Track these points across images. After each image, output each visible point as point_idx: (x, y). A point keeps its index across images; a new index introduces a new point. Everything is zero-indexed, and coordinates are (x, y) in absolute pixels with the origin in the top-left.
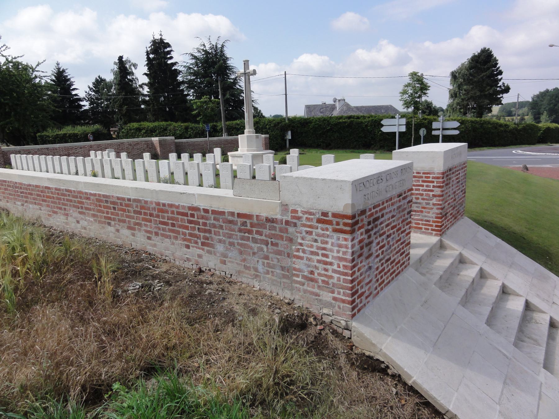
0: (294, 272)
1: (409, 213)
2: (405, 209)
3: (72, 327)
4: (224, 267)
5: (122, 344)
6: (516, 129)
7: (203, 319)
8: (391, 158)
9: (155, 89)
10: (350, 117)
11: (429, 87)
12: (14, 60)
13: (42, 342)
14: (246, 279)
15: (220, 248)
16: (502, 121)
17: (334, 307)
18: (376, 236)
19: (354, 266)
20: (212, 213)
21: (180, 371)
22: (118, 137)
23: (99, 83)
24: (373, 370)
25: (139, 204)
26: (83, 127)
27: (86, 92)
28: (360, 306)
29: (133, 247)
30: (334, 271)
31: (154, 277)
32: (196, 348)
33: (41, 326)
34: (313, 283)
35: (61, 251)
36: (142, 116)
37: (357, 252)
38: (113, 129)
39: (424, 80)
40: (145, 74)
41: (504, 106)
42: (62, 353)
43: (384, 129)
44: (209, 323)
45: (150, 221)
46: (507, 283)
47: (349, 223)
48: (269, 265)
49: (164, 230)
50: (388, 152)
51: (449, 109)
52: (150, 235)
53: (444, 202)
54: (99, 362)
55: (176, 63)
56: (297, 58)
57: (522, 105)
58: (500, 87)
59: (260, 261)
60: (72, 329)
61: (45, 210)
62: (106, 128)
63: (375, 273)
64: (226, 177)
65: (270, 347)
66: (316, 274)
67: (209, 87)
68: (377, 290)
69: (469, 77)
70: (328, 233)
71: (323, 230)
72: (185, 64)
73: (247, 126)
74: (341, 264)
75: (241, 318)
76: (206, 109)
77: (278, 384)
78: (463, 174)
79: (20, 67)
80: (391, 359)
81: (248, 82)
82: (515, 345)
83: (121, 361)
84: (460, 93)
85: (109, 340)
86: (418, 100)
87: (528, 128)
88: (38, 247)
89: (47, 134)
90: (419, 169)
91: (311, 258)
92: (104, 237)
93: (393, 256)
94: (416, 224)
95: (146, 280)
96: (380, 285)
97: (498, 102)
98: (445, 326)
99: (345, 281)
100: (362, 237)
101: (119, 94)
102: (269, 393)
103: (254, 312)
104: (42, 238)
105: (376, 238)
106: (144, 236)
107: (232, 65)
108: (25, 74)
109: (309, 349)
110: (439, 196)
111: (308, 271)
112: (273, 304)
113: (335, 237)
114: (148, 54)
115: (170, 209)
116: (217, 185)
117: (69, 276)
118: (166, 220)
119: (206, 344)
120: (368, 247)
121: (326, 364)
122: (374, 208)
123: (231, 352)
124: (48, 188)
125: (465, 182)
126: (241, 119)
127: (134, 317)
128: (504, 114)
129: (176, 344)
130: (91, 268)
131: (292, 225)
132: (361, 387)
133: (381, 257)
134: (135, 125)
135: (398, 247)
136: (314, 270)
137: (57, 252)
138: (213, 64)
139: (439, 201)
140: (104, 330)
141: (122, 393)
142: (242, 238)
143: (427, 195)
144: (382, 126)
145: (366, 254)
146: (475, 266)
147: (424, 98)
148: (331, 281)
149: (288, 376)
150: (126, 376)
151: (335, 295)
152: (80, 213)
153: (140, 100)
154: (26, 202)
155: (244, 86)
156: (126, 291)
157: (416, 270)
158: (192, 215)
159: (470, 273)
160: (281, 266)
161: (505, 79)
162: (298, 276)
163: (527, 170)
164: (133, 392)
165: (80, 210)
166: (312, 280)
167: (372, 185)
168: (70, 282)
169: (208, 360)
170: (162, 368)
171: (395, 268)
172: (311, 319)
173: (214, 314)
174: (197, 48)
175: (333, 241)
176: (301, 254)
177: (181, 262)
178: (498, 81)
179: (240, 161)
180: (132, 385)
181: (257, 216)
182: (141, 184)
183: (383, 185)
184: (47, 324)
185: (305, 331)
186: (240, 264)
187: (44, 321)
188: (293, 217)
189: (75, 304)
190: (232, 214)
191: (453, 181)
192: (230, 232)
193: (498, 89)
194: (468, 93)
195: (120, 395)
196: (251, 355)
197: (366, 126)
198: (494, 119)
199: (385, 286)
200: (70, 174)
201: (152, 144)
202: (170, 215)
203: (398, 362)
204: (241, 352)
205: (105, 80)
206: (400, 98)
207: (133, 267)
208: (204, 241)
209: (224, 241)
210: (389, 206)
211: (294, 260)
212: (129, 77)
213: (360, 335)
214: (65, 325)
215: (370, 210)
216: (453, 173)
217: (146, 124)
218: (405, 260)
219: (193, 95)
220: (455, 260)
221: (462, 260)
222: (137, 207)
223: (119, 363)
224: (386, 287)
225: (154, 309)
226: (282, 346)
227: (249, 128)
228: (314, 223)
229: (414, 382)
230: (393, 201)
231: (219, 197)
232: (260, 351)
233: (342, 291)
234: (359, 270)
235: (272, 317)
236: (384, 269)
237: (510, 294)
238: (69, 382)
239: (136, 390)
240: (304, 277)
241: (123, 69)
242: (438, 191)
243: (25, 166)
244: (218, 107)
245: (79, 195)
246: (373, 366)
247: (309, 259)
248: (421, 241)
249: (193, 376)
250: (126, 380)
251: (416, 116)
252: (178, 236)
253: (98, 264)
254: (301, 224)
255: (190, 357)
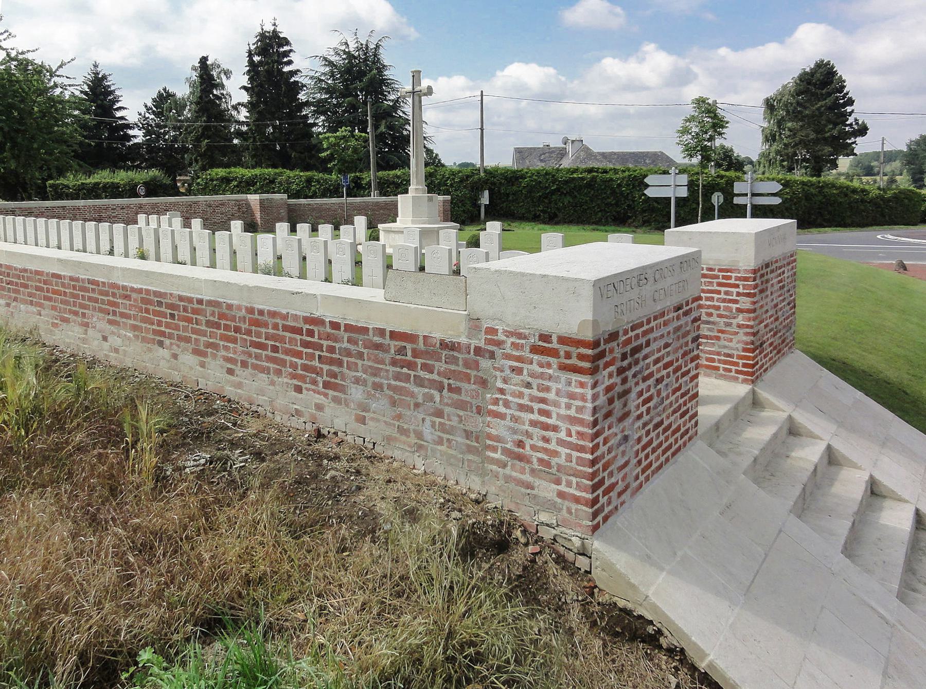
0: (489, 442)
1: (695, 339)
2: (688, 332)
3: (74, 536)
4: (361, 429)
5: (164, 571)
6: (882, 198)
7: (318, 527)
8: (662, 243)
9: (259, 112)
10: (590, 171)
11: (727, 123)
12: (20, 57)
13: (13, 564)
14: (399, 453)
15: (356, 393)
16: (856, 184)
17: (560, 510)
18: (636, 380)
19: (597, 435)
20: (346, 331)
21: (270, 626)
22: (189, 192)
23: (164, 100)
24: (633, 638)
25: (216, 310)
26: (130, 173)
27: (140, 114)
28: (607, 510)
29: (200, 387)
30: (561, 442)
31: (233, 445)
32: (303, 583)
33: (15, 532)
34: (522, 464)
35: (68, 391)
36: (234, 158)
37: (602, 408)
38: (182, 178)
39: (719, 111)
40: (244, 88)
41: (858, 157)
42: (48, 587)
43: (650, 193)
44: (328, 534)
45: (234, 341)
46: (878, 476)
47: (588, 356)
48: (443, 428)
49: (258, 357)
50: (656, 232)
51: (762, 160)
52: (233, 367)
53: (757, 322)
54: (118, 606)
55: (298, 71)
56: (502, 70)
57: (890, 157)
58: (851, 125)
59: (428, 419)
60: (73, 541)
61: (47, 315)
62: (169, 176)
63: (635, 449)
64: (372, 267)
65: (440, 584)
66: (528, 447)
67: (351, 113)
68: (639, 481)
69: (795, 108)
70: (550, 371)
71: (541, 366)
72: (312, 74)
73: (413, 180)
74: (574, 429)
75: (387, 527)
76: (344, 149)
77: (451, 660)
78: (790, 274)
79: (30, 67)
80: (667, 617)
81: (418, 107)
82: (901, 597)
83: (160, 606)
84: (781, 134)
85: (141, 564)
86: (709, 144)
87: (903, 196)
88: (28, 383)
89: (66, 182)
90: (711, 262)
91: (520, 417)
92: (150, 367)
93: (668, 418)
94: (708, 359)
95: (219, 449)
96: (643, 471)
97: (848, 150)
98: (766, 555)
99: (580, 461)
100: (612, 381)
101: (196, 119)
102: (434, 676)
103: (412, 515)
104: (37, 366)
105: (637, 384)
106: (222, 367)
107: (391, 77)
108: (37, 80)
109: (511, 590)
110: (749, 311)
111: (514, 442)
112: (449, 501)
113: (563, 379)
114: (250, 55)
115: (271, 321)
116: (357, 281)
117: (79, 437)
118: (263, 340)
119: (321, 575)
120: (623, 400)
121: (545, 622)
122: (633, 328)
123: (367, 592)
124: (59, 276)
125: (794, 287)
126: (403, 168)
127: (192, 518)
128: (859, 171)
129: (265, 574)
130: (120, 425)
131: (487, 355)
132: (610, 671)
133: (646, 418)
134: (221, 172)
135: (677, 401)
136: (524, 439)
137: (62, 392)
138: (360, 76)
139: (749, 320)
140: (133, 542)
141: (156, 669)
142: (397, 377)
143: (726, 308)
144: (647, 186)
145: (618, 413)
146: (819, 441)
147: (718, 142)
148: (554, 461)
149: (472, 644)
150: (166, 635)
151: (563, 488)
152: (111, 322)
153: (232, 130)
154: (15, 299)
155: (411, 114)
156: (180, 469)
157: (710, 445)
158: (311, 333)
159: (809, 454)
160: (465, 430)
161: (859, 112)
162: (495, 449)
163: (905, 269)
164: (177, 670)
165: (110, 317)
166: (520, 458)
167: (628, 288)
168: (78, 449)
169: (322, 608)
170: (236, 622)
171: (671, 440)
172: (518, 533)
173: (339, 517)
174: (335, 49)
175: (560, 386)
176: (501, 409)
177: (286, 417)
178: (846, 115)
179: (399, 240)
180: (177, 654)
181: (425, 337)
182: (223, 274)
183: (648, 289)
184: (28, 528)
185: (506, 556)
186: (390, 424)
187: (22, 523)
188: (489, 342)
189: (83, 491)
190: (381, 332)
191: (772, 285)
192: (376, 365)
193: (847, 129)
194: (795, 134)
195: (151, 675)
196: (403, 599)
197: (619, 185)
198: (842, 179)
199: (653, 473)
200: (98, 252)
201: (248, 205)
202: (271, 331)
203: (680, 623)
204: (385, 593)
205: (174, 95)
206: (678, 140)
207: (198, 424)
208: (328, 379)
209: (365, 381)
210: (658, 327)
211: (489, 419)
212: (215, 92)
213: (608, 567)
214: (62, 530)
215: (626, 332)
216: (772, 271)
217: (239, 171)
218: (688, 425)
219: (323, 125)
220: (781, 428)
221: (793, 430)
222: (213, 314)
223: (155, 608)
224: (655, 476)
225: (229, 505)
226: (463, 585)
227: (417, 184)
228: (526, 353)
229: (711, 665)
230: (666, 318)
231: (359, 302)
232: (420, 591)
233: (574, 480)
234: (605, 441)
235: (444, 526)
236: (650, 442)
237: (885, 497)
238: (56, 646)
239: (183, 664)
240: (506, 451)
241: (207, 77)
242: (745, 303)
243: (20, 237)
244: (365, 147)
245: (111, 290)
246: (633, 630)
247: (515, 419)
248: (718, 392)
249: (292, 638)
250: (166, 643)
251: (706, 171)
252: (283, 369)
253: (135, 416)
254: (503, 354)
255: (290, 600)
